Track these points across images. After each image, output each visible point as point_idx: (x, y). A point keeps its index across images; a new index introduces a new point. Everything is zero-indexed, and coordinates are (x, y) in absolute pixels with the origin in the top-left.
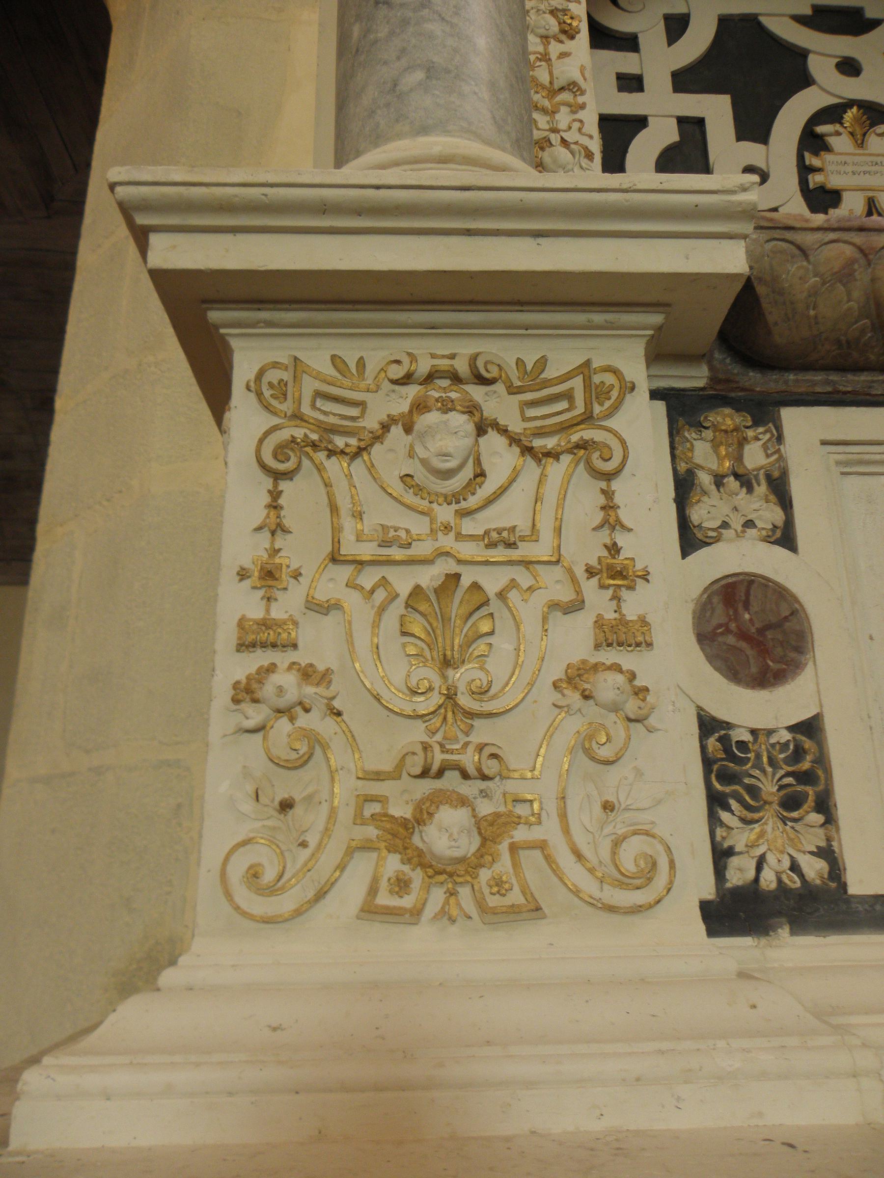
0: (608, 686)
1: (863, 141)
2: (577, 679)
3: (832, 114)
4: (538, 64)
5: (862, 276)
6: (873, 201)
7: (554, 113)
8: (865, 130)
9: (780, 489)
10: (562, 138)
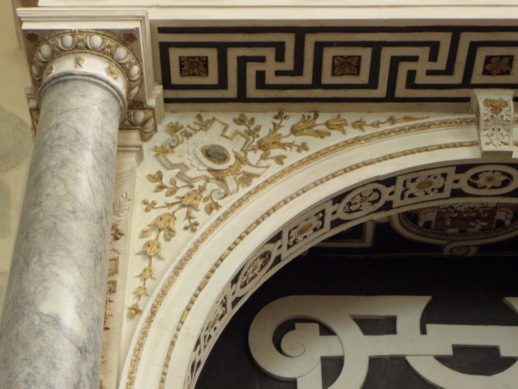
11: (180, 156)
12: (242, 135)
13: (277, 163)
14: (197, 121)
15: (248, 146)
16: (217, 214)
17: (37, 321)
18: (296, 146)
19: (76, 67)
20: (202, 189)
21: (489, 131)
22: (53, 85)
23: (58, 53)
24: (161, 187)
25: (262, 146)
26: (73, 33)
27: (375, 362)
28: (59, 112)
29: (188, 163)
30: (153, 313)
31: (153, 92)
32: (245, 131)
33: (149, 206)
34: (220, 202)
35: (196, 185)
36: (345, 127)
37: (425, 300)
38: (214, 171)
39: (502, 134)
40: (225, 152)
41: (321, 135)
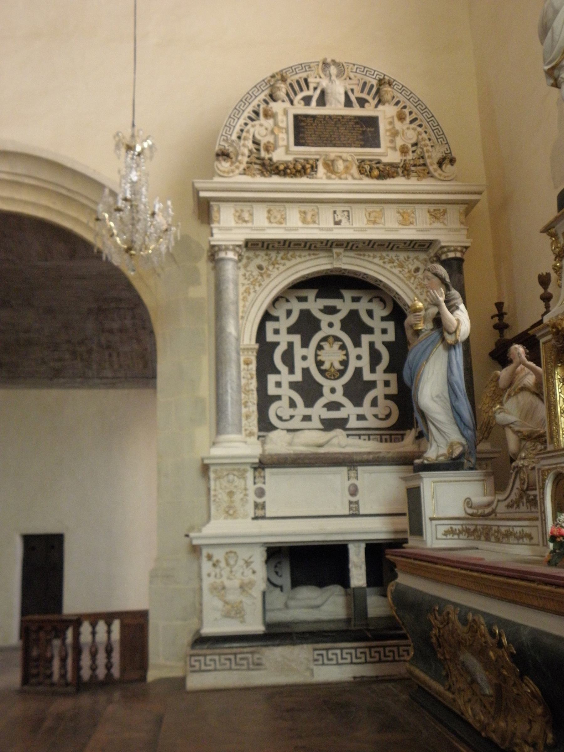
0: (245, 500)
2: (242, 499)
3: (325, 339)
9: (264, 477)
16: (262, 288)
20: (257, 279)
24: (246, 279)
25: (273, 264)
33: (243, 285)
41: (289, 260)
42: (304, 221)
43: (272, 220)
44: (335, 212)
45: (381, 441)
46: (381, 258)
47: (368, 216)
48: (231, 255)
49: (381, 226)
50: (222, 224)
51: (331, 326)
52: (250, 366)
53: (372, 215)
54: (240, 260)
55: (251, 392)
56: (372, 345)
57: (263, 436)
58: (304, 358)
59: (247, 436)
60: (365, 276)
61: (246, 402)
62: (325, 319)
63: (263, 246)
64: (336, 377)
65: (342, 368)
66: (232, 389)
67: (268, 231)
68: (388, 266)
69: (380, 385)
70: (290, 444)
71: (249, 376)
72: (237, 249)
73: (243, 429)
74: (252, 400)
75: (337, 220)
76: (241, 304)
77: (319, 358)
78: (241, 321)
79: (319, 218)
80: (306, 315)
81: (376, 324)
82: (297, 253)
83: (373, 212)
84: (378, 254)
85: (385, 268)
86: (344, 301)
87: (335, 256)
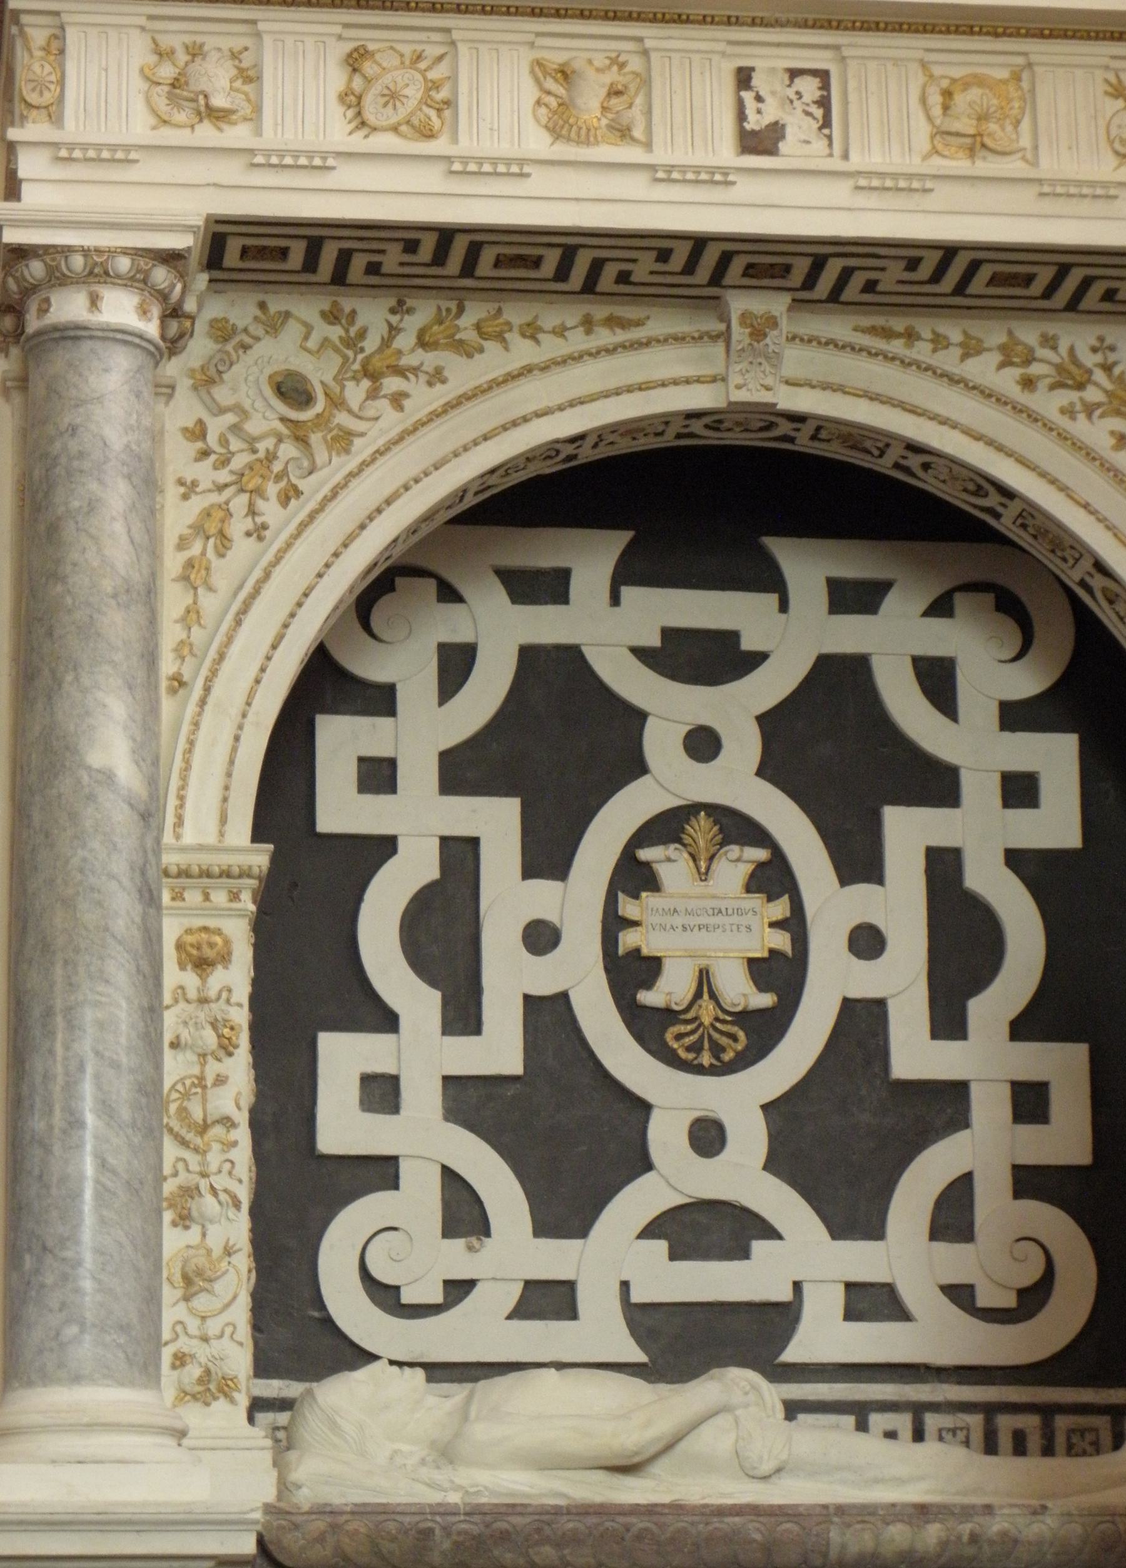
1: (708, 869)
3: (667, 827)
4: (194, 1090)
5: (331, 1540)
6: (707, 972)
7: (205, 1152)
8: (713, 850)
10: (212, 1186)
11: (234, 390)
12: (337, 350)
13: (395, 408)
14: (258, 313)
15: (346, 372)
16: (300, 510)
17: (86, 779)
18: (427, 373)
19: (92, 312)
20: (271, 457)
21: (744, 365)
22: (56, 340)
23: (58, 279)
24: (205, 454)
26: (85, 252)
27: (529, 655)
28: (72, 402)
29: (247, 404)
30: (207, 689)
31: (193, 287)
32: (340, 338)
33: (189, 489)
34: (302, 485)
35: (262, 446)
36: (506, 335)
37: (624, 537)
38: (291, 421)
39: (764, 372)
40: (309, 387)
41: (467, 350)
42: (562, 123)
43: (371, 114)
44: (744, 78)
45: (990, 1447)
46: (1009, 356)
47: (937, 111)
48: (121, 309)
49: (1013, 167)
50: (75, 127)
51: (703, 749)
52: (218, 978)
53: (961, 100)
54: (173, 345)
55: (218, 1131)
56: (943, 865)
57: (285, 1405)
58: (541, 937)
59: (184, 1395)
60: (914, 461)
61: (190, 1192)
62: (670, 708)
63: (311, 263)
64: (728, 1056)
65: (766, 1000)
66: (106, 1109)
67: (348, 175)
68: (1049, 403)
69: (989, 1107)
70: (446, 1453)
71: (210, 1038)
72: (161, 275)
73: (167, 1354)
74: (220, 1182)
75: (754, 122)
76: (173, 601)
77: (628, 940)
78: (167, 705)
79: (648, 112)
80: (555, 680)
81: (970, 743)
82: (516, 313)
83: (967, 84)
84: (994, 333)
85: (1034, 418)
86: (784, 607)
87: (739, 333)
